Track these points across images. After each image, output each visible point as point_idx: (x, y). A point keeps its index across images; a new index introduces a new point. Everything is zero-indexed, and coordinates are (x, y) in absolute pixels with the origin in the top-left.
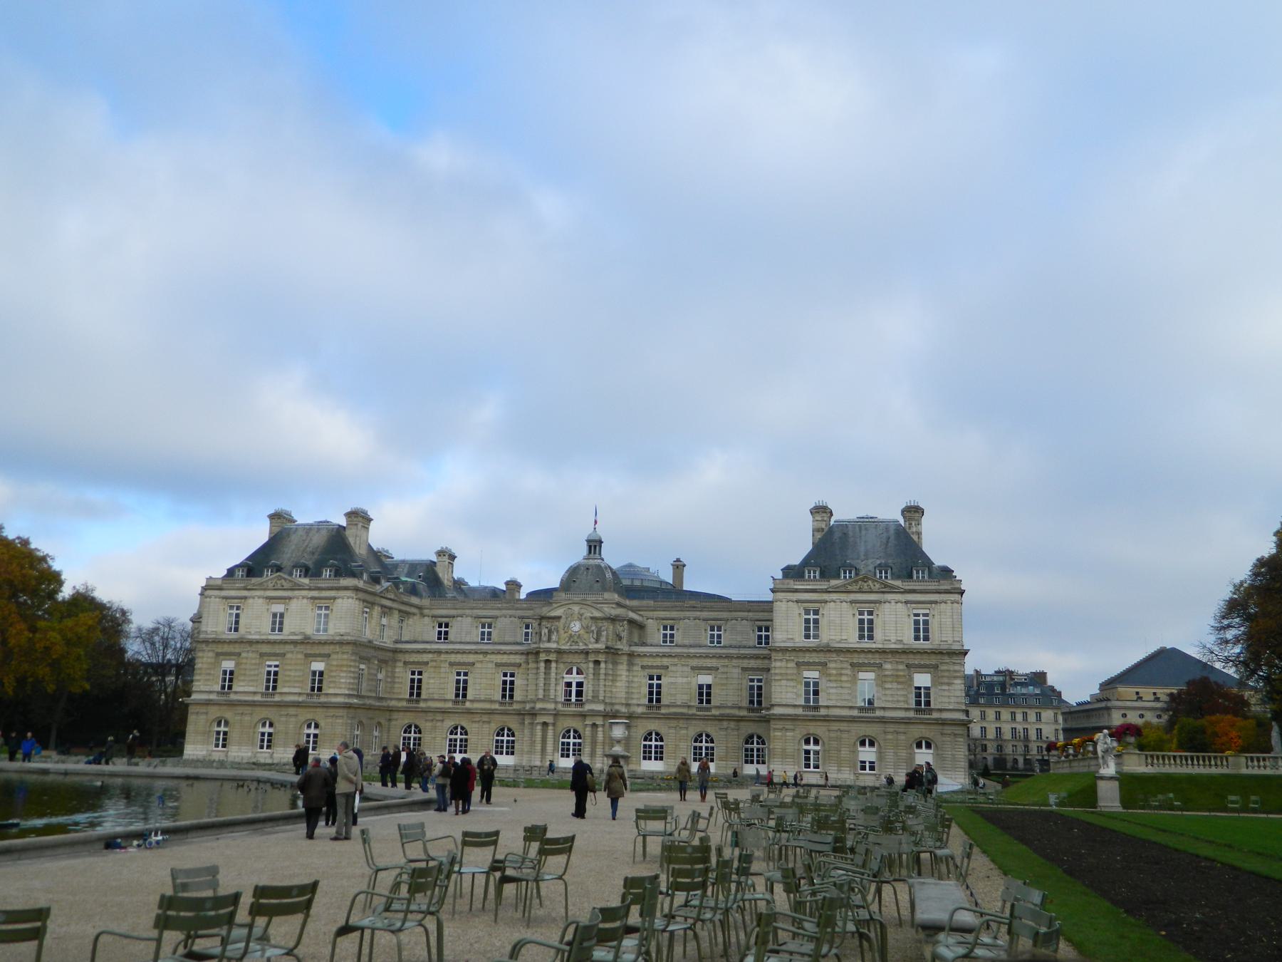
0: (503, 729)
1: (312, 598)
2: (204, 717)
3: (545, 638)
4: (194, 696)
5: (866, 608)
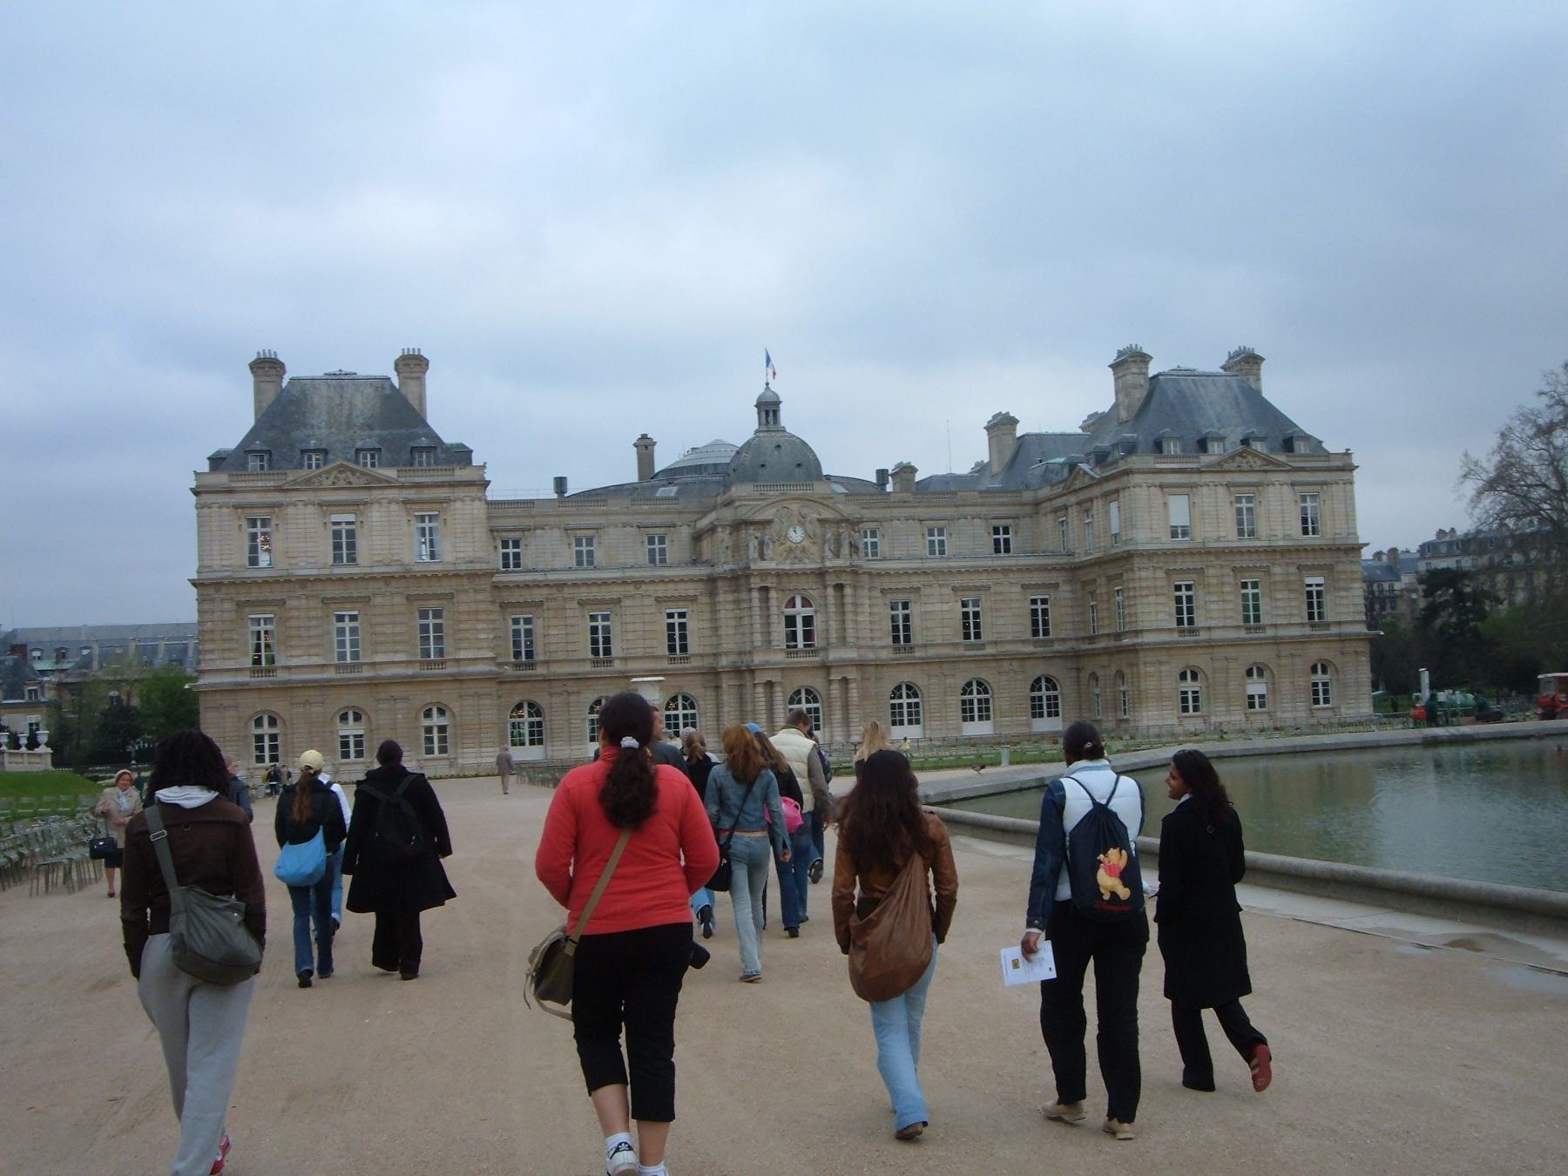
0: (674, 699)
1: (405, 502)
4: (201, 682)
5: (1246, 492)
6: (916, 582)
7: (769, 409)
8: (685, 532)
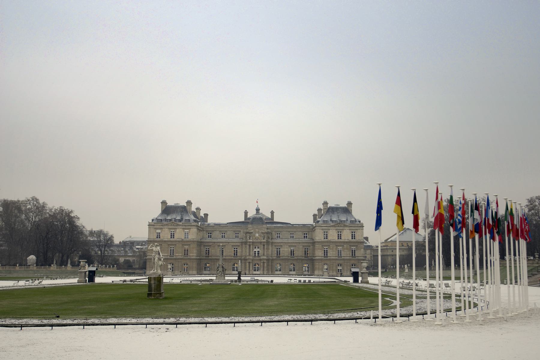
6: (282, 244)
7: (258, 210)
8: (242, 232)
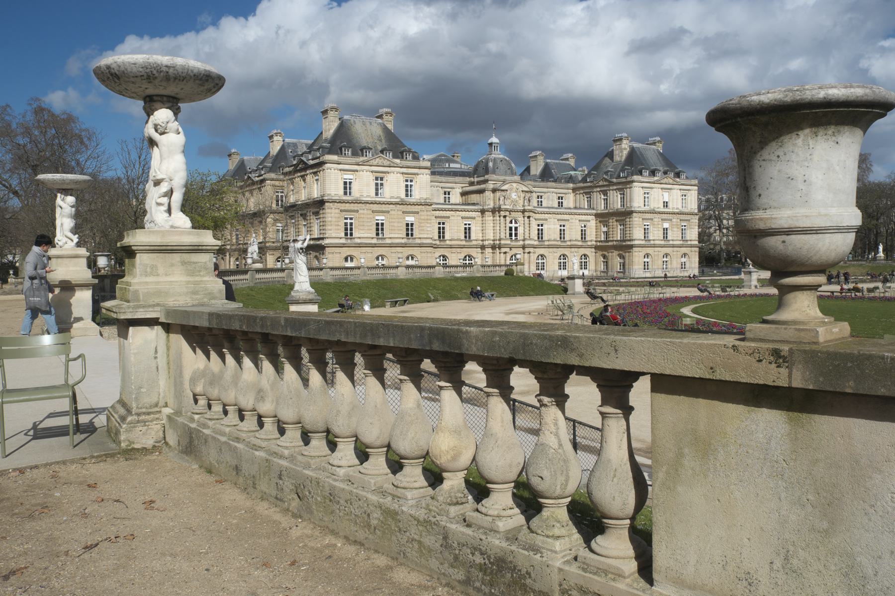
2: (338, 255)
3: (501, 202)
